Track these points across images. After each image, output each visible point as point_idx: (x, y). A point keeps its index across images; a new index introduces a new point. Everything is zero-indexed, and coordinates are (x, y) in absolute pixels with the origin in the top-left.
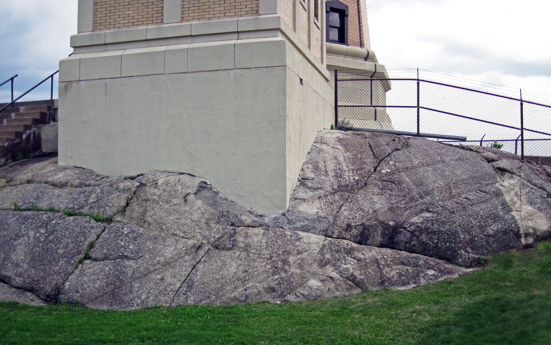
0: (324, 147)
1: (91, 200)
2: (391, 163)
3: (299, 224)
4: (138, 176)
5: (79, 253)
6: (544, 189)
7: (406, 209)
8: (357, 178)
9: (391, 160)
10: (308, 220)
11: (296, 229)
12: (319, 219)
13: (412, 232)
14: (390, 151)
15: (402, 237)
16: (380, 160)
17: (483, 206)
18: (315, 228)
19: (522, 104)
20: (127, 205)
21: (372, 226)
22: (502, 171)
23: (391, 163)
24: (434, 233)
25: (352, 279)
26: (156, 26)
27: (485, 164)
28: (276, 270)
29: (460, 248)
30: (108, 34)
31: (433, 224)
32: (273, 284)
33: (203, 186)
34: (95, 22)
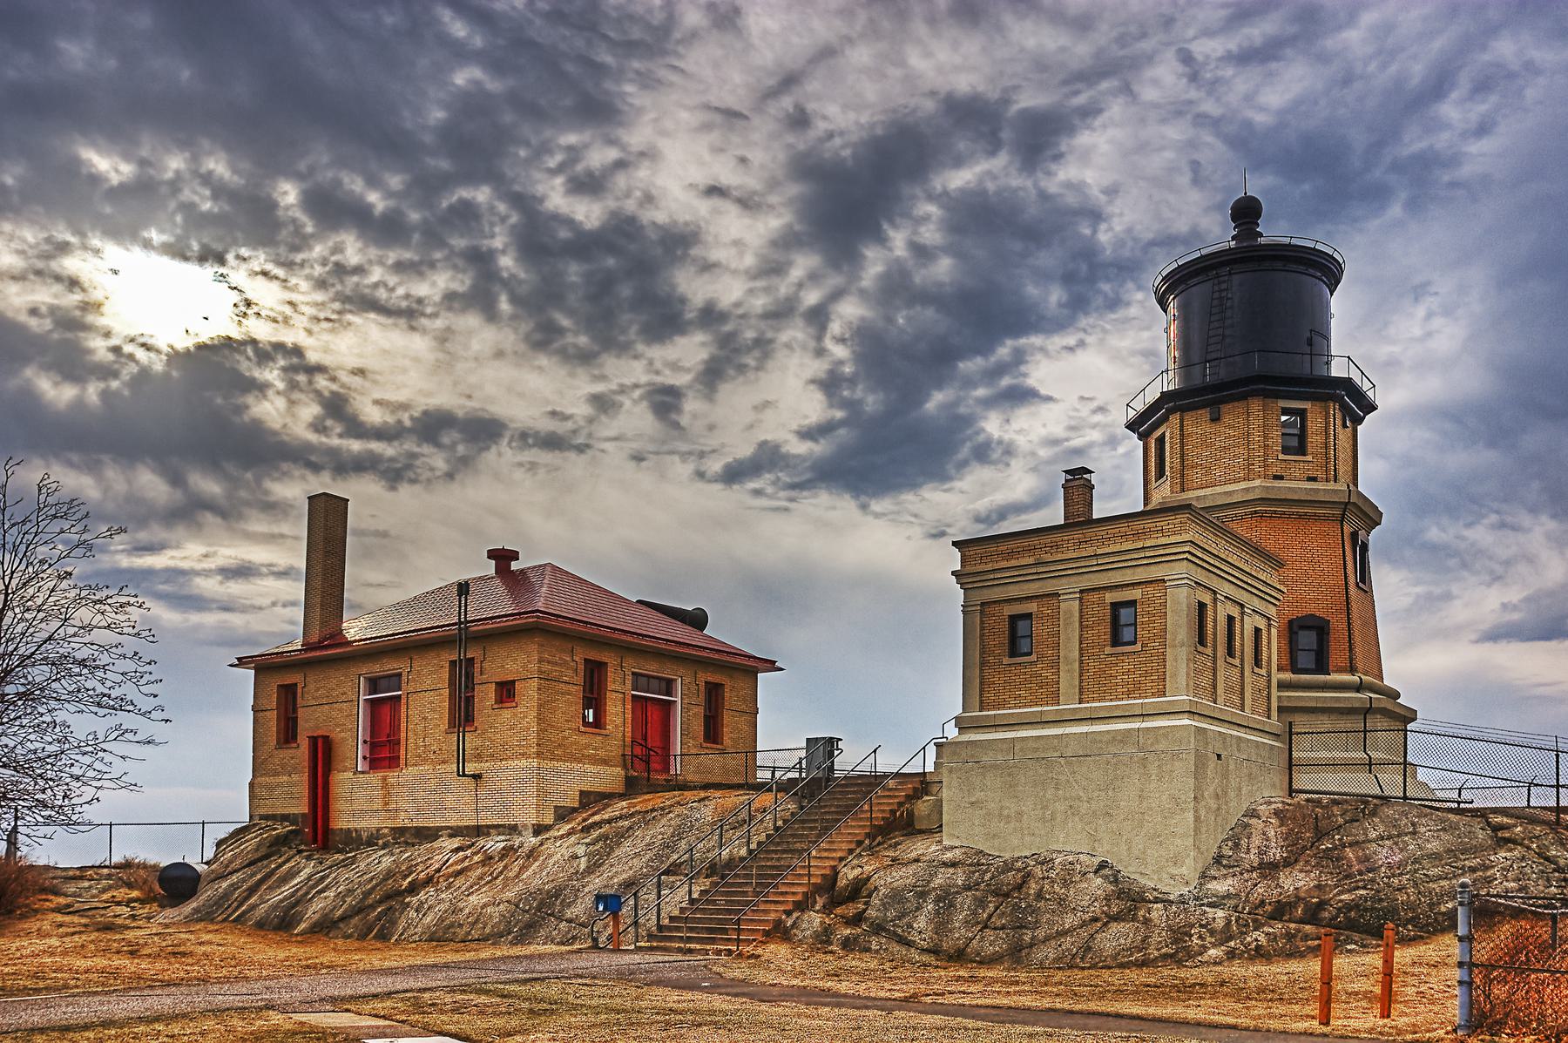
0: (1253, 821)
1: (986, 878)
2: (1337, 837)
3: (1205, 901)
5: (978, 923)
7: (1336, 886)
8: (1285, 855)
9: (1338, 834)
10: (1217, 897)
11: (1203, 905)
12: (1228, 896)
13: (1339, 909)
16: (1320, 835)
17: (1444, 883)
20: (1024, 882)
21: (1290, 903)
23: (1337, 837)
24: (1366, 910)
28: (1176, 941)
31: (1366, 901)
33: (1103, 865)
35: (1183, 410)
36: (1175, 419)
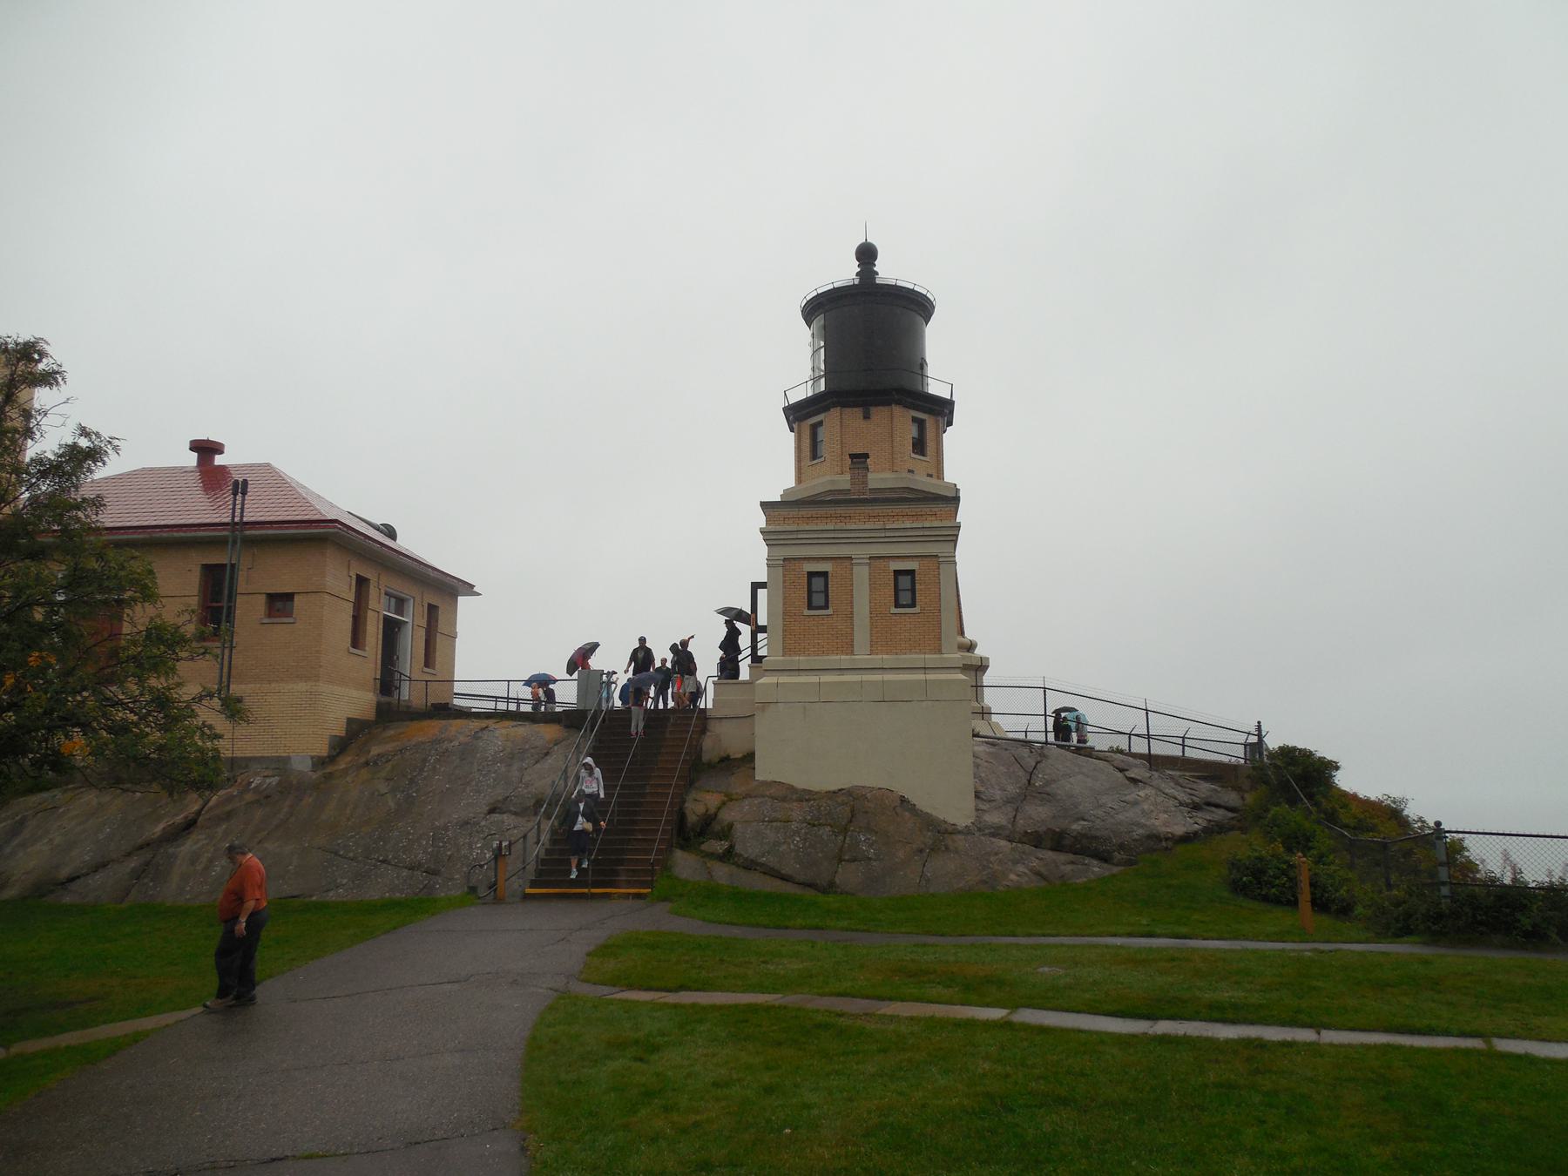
3: (987, 831)
4: (840, 790)
6: (1176, 799)
9: (1039, 773)
10: (993, 827)
13: (1075, 837)
14: (1034, 764)
15: (1067, 842)
18: (1000, 834)
19: (1147, 713)
22: (1134, 781)
25: (1038, 874)
26: (848, 657)
27: (1119, 775)
29: (1114, 851)
30: (802, 660)
32: (984, 878)
34: (784, 648)
35: (844, 405)
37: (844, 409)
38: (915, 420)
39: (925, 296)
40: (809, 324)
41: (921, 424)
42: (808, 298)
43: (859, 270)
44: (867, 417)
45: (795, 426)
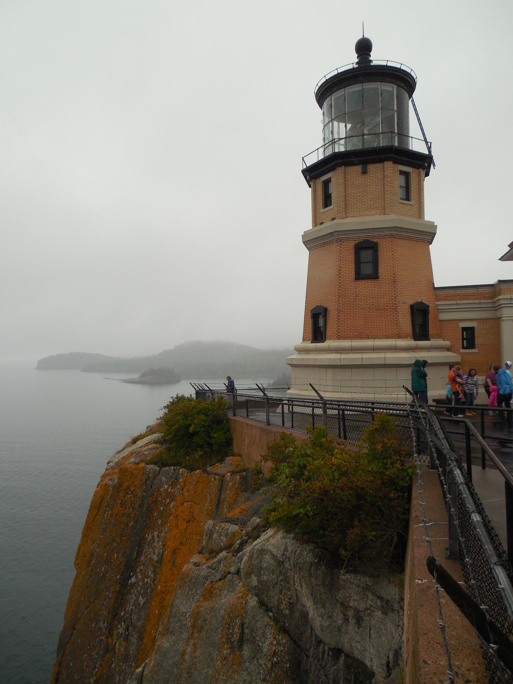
36: (340, 170)
37: (347, 168)
38: (402, 173)
39: (410, 74)
40: (321, 106)
41: (407, 175)
42: (319, 85)
43: (358, 60)
44: (364, 172)
45: (312, 184)
